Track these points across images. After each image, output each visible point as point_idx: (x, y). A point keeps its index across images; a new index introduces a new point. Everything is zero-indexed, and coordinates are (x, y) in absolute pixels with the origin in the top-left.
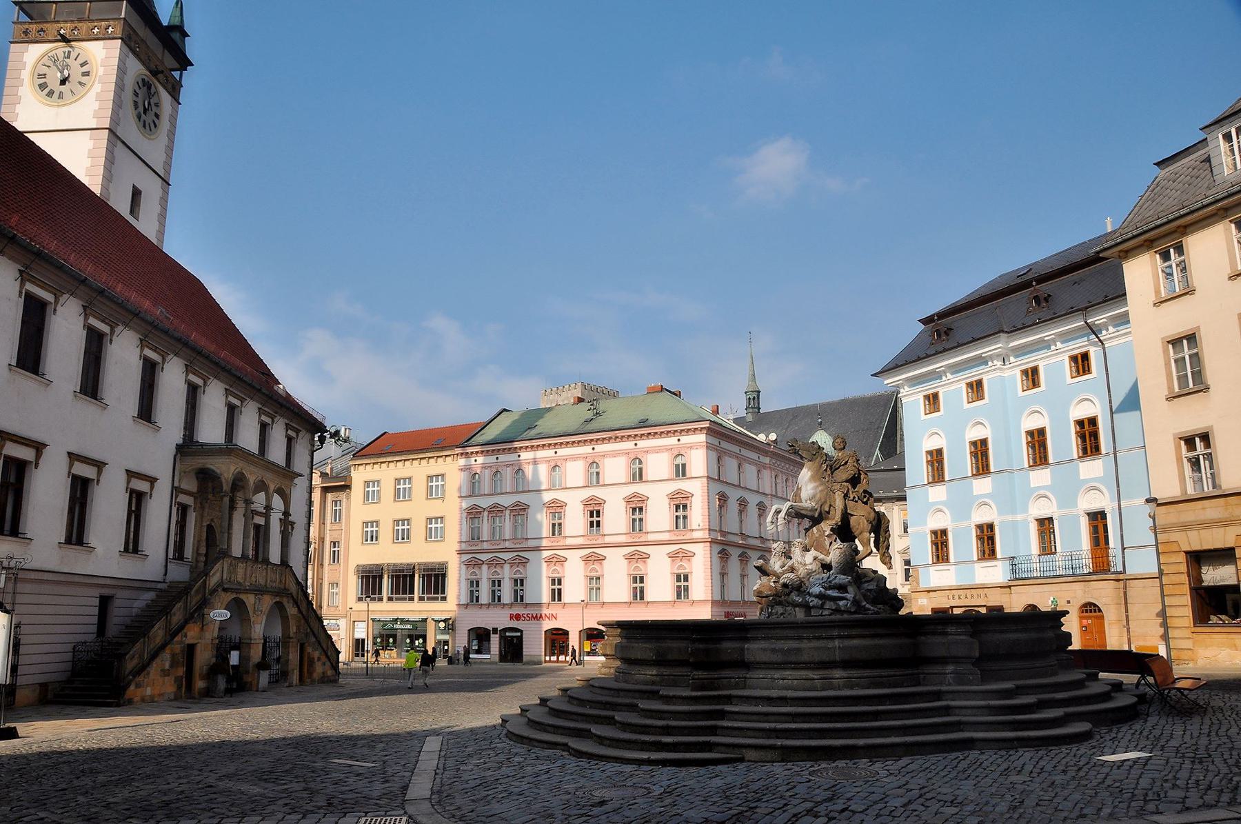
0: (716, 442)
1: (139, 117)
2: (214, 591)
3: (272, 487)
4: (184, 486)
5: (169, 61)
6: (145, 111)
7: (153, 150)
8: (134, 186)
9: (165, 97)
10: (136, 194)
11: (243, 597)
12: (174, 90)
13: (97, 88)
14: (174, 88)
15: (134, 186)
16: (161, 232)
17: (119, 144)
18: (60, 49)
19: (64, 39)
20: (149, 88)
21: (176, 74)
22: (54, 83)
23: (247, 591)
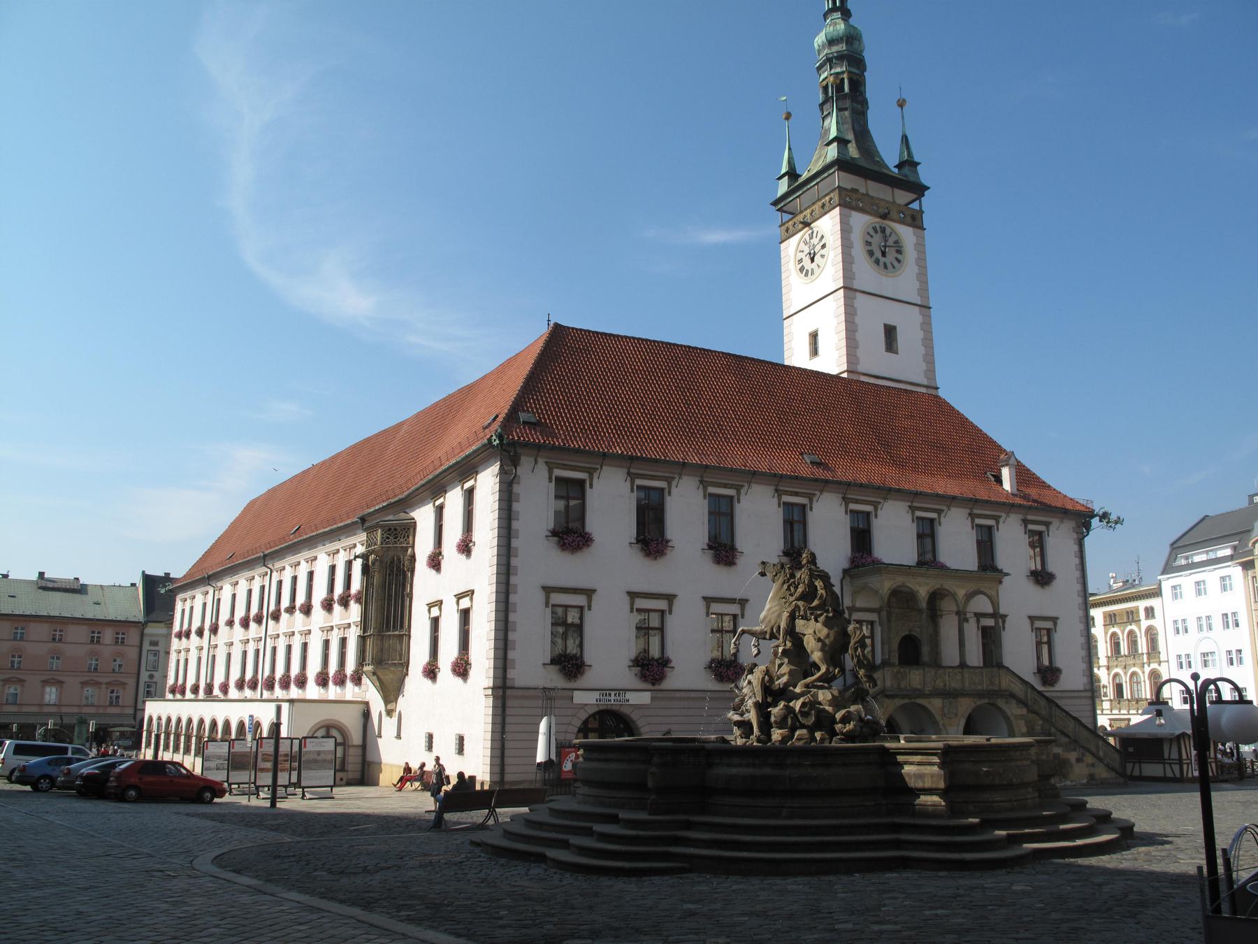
1: (877, 262)
3: (961, 593)
4: (858, 604)
5: (902, 197)
6: (884, 254)
7: (904, 283)
8: (885, 326)
9: (905, 233)
10: (890, 332)
12: (915, 220)
14: (913, 218)
15: (885, 326)
17: (858, 294)
18: (805, 233)
19: (807, 224)
20: (883, 230)
21: (915, 206)
22: (807, 263)
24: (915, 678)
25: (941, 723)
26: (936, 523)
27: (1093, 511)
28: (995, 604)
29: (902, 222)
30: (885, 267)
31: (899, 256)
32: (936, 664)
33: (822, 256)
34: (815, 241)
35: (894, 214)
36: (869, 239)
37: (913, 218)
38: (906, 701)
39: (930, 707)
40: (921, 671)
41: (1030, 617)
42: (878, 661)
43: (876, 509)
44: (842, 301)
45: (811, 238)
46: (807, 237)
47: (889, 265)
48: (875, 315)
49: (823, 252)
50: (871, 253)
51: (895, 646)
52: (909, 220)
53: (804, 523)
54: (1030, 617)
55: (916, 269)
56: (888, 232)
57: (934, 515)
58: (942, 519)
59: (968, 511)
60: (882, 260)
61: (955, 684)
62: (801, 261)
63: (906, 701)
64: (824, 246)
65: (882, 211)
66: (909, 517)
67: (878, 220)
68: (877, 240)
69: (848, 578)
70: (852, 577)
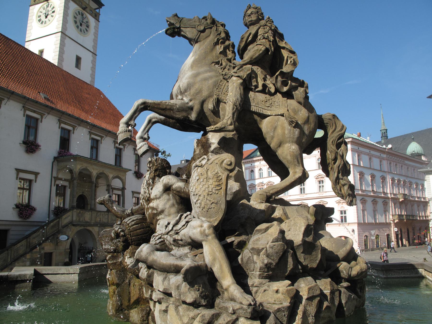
0: (356, 148)
2: (66, 226)
3: (111, 176)
4: (60, 176)
6: (81, 25)
7: (88, 40)
8: (77, 56)
9: (92, 20)
10: (78, 59)
11: (90, 228)
12: (96, 16)
13: (57, 16)
14: (96, 16)
15: (77, 56)
16: (93, 76)
17: (67, 38)
20: (82, 15)
21: (97, 11)
22: (43, 18)
23: (90, 225)
24: (87, 216)
25: (97, 239)
26: (99, 142)
27: (159, 150)
28: (124, 183)
29: (91, 15)
30: (81, 31)
31: (87, 28)
32: (93, 210)
33: (52, 16)
34: (49, 9)
35: (88, 9)
36: (76, 16)
37: (96, 16)
38: (82, 228)
39: (93, 232)
40: (90, 213)
41: (132, 192)
42: (67, 206)
43: (74, 129)
44: (59, 38)
45: (48, 7)
46: (45, 6)
47: (82, 30)
48: (73, 50)
49: (53, 14)
50: (76, 22)
51: (75, 199)
52: (94, 15)
53: (36, 129)
54: (132, 192)
55: (93, 37)
56: (84, 16)
57: (99, 138)
58: (102, 141)
59: (114, 140)
60: (80, 27)
61: (105, 220)
62: (40, 16)
63: (82, 228)
64: (54, 12)
65: (84, 6)
66: (88, 136)
67: (81, 9)
68: (79, 17)
69: (56, 161)
70: (58, 162)
